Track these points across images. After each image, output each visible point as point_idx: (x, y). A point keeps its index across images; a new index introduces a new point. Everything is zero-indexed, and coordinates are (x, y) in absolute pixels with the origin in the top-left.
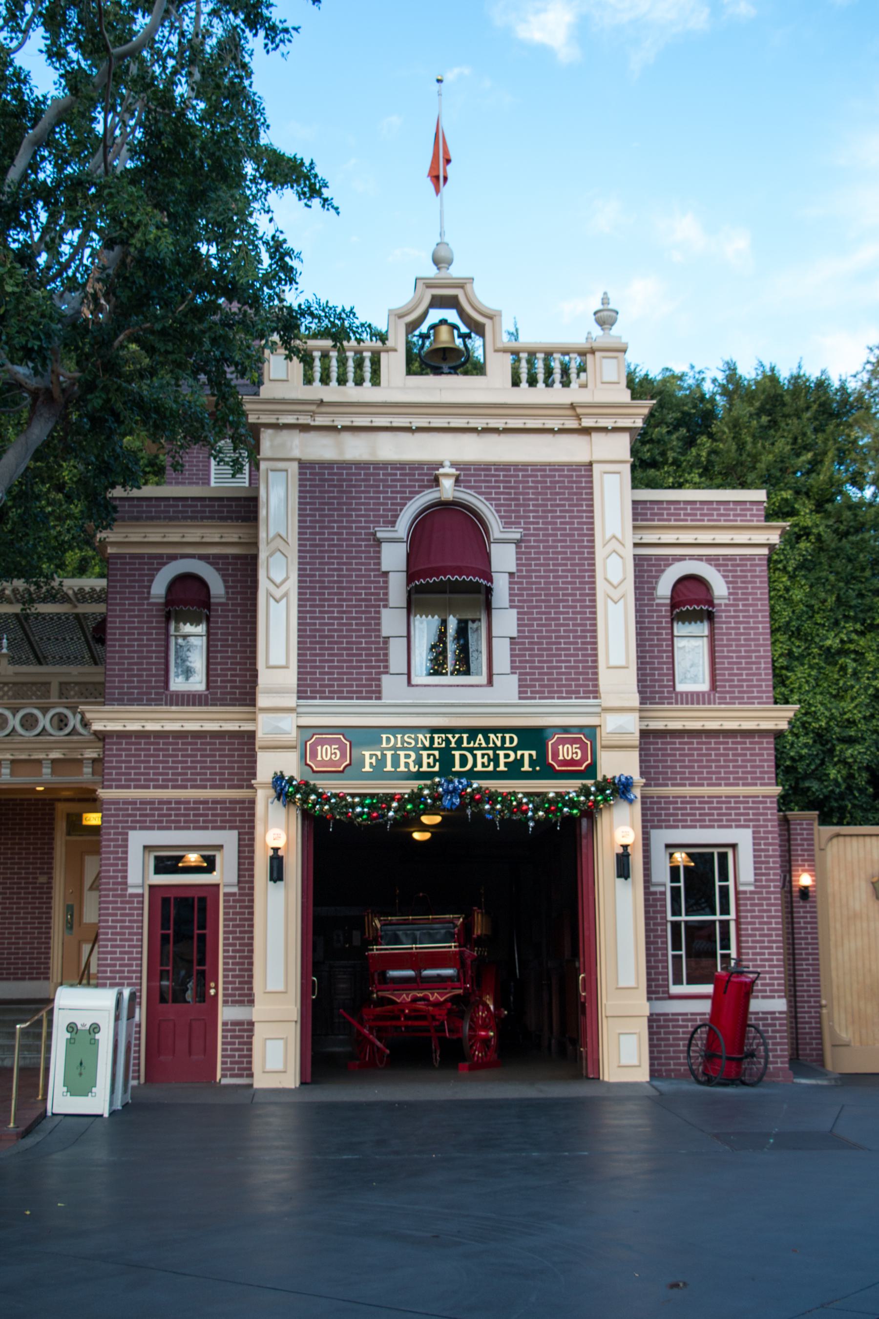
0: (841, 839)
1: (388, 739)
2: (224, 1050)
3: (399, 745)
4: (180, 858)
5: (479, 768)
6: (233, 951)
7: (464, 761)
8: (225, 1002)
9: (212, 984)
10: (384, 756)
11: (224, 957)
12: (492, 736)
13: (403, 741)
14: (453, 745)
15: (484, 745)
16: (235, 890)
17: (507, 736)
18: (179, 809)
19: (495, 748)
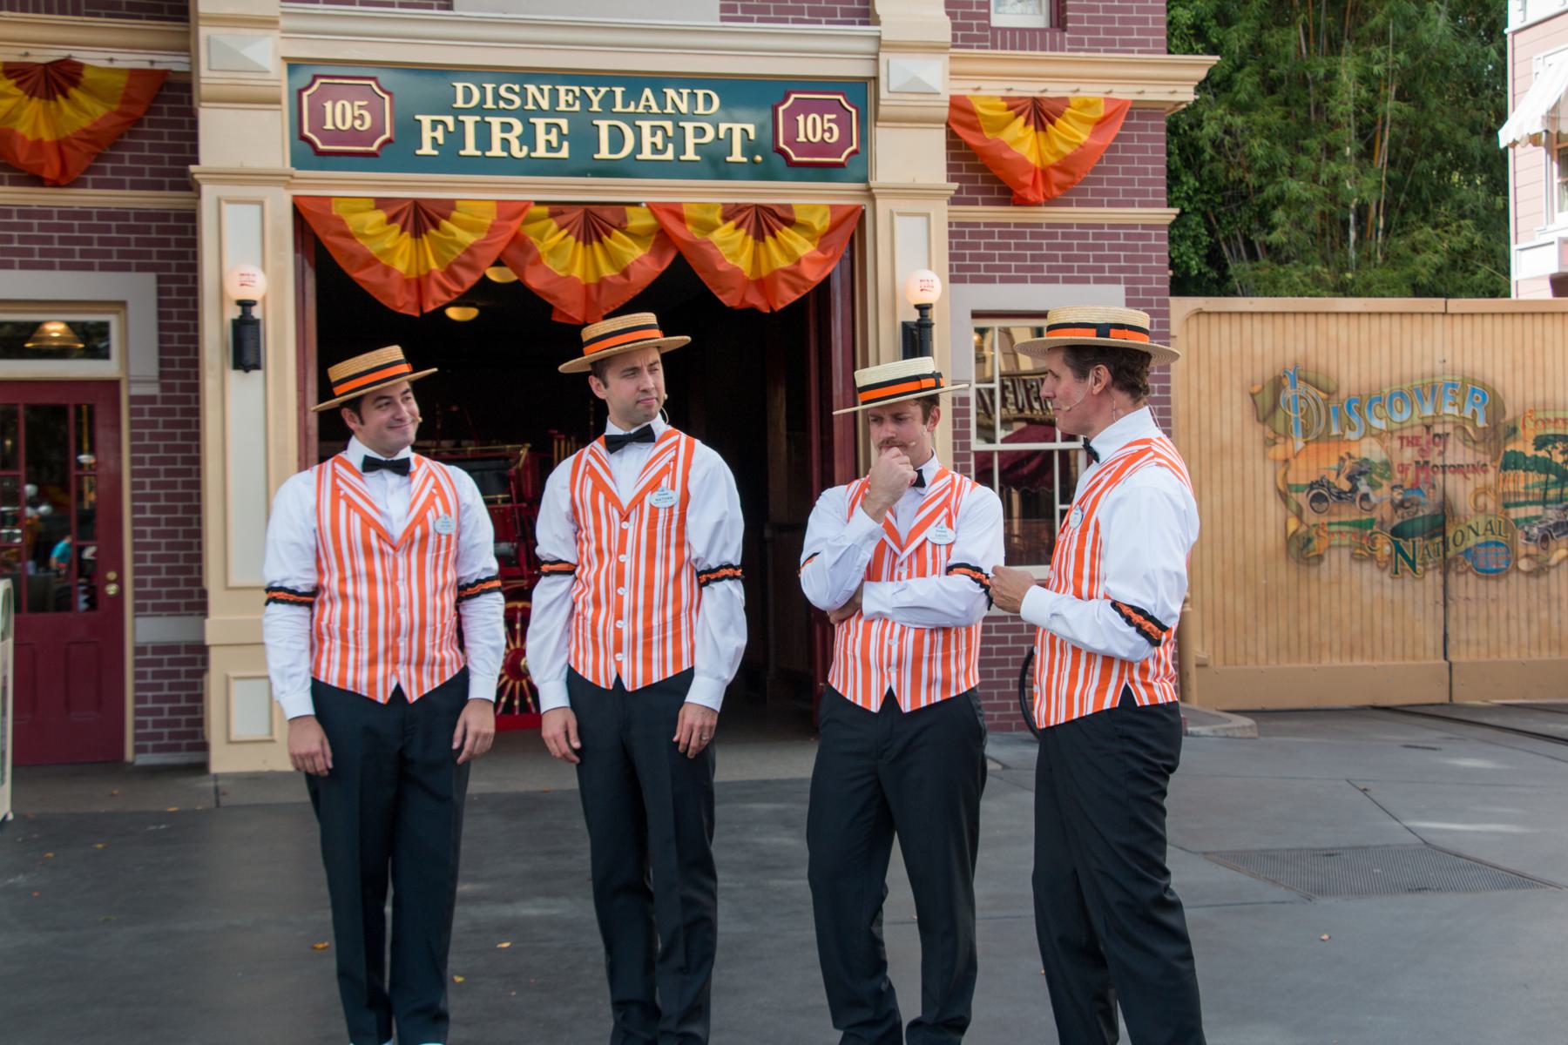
0: (1203, 319)
1: (468, 96)
2: (138, 700)
3: (490, 104)
4: (36, 326)
5: (647, 154)
6: (155, 510)
7: (617, 140)
8: (139, 609)
9: (112, 575)
10: (460, 125)
11: (135, 522)
12: (671, 93)
13: (497, 97)
14: (596, 108)
15: (655, 109)
16: (154, 390)
17: (700, 93)
18: (29, 227)
19: (677, 117)
